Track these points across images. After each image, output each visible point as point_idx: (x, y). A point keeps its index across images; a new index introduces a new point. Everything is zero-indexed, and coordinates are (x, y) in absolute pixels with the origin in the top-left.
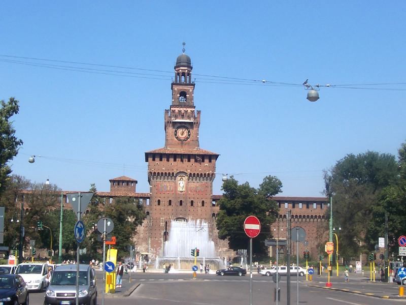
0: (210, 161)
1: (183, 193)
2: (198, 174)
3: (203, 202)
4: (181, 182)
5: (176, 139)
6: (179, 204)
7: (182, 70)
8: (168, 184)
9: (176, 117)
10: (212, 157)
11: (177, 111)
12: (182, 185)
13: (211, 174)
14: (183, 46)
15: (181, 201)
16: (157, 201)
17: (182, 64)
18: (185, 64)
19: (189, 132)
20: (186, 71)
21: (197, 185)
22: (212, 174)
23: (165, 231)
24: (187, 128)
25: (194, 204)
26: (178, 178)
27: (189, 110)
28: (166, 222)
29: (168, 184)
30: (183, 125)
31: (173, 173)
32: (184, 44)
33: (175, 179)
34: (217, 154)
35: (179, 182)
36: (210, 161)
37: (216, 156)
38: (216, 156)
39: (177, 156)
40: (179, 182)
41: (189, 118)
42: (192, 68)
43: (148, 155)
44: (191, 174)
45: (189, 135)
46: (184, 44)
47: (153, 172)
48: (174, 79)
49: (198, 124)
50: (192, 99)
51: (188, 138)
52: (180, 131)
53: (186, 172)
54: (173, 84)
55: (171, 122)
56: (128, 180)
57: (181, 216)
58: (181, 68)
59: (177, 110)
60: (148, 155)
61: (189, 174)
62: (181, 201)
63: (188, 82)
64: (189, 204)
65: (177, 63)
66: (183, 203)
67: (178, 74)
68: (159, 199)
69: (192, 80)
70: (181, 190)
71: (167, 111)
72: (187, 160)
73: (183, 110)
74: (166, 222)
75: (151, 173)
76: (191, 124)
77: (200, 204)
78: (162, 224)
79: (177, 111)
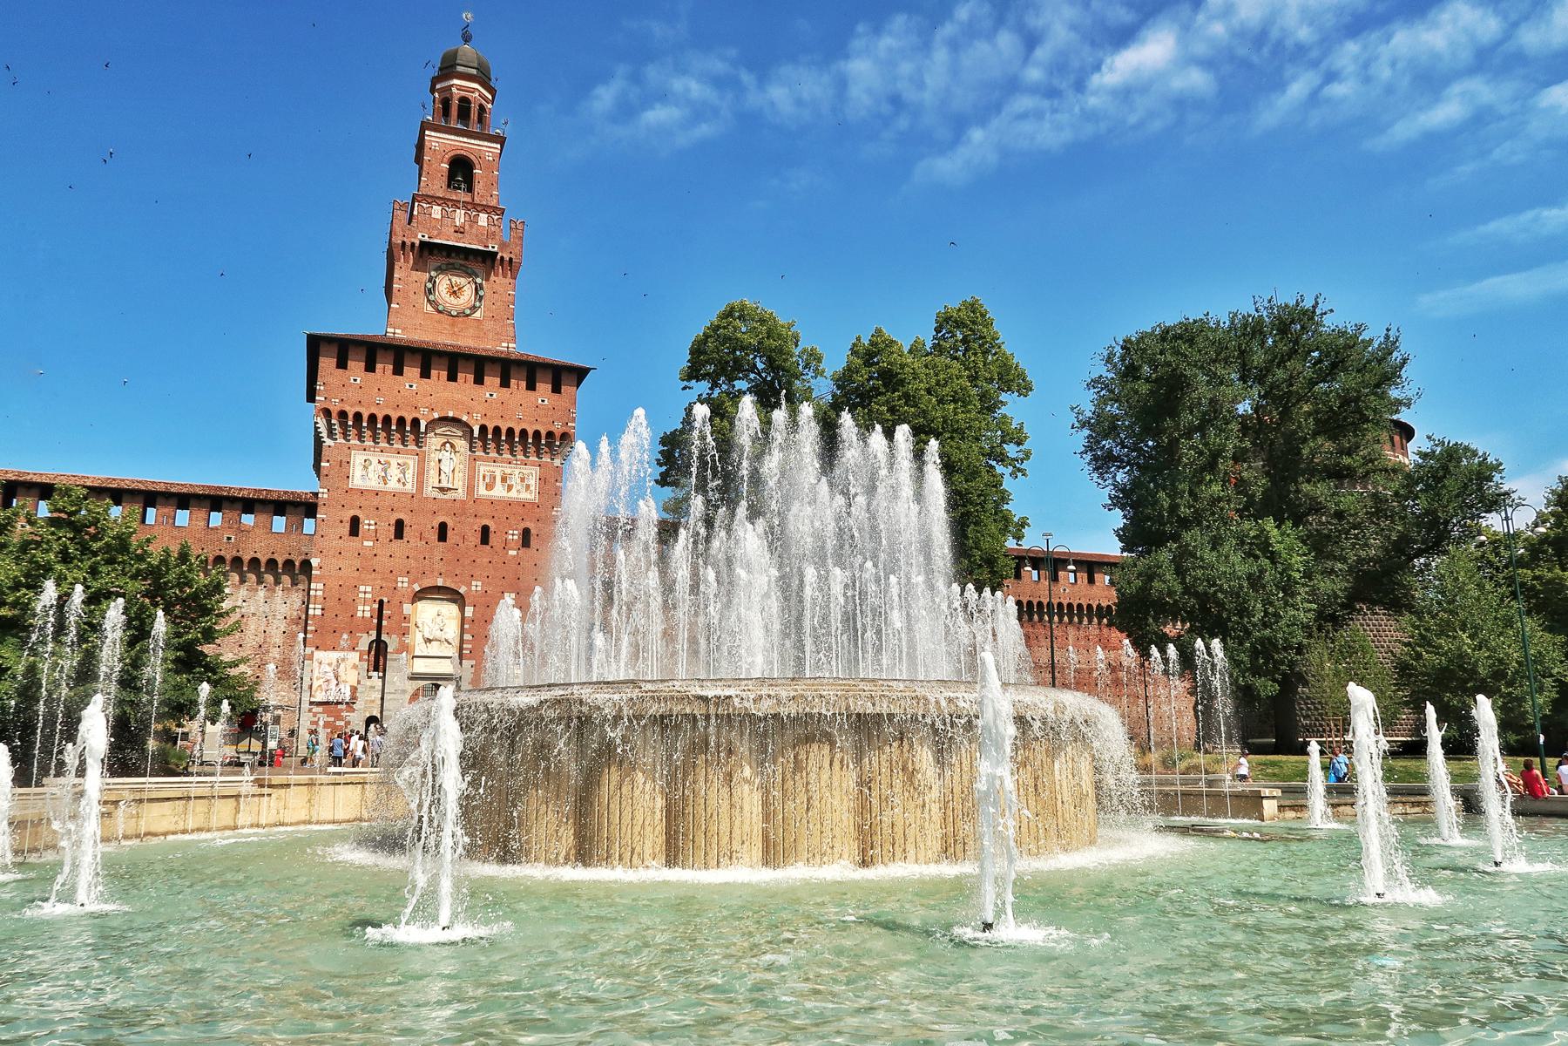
1: (449, 496)
2: (510, 431)
3: (526, 534)
4: (445, 455)
7: (460, 88)
10: (564, 376)
12: (446, 467)
13: (558, 435)
15: (443, 528)
16: (347, 518)
17: (460, 69)
19: (478, 288)
24: (470, 274)
25: (493, 538)
26: (433, 442)
27: (483, 219)
28: (381, 603)
30: (463, 262)
31: (416, 422)
33: (418, 443)
35: (436, 456)
36: (556, 389)
37: (580, 374)
38: (580, 374)
39: (435, 360)
40: (436, 456)
43: (315, 345)
44: (483, 429)
49: (511, 266)
51: (474, 308)
52: (443, 283)
53: (465, 418)
54: (424, 126)
55: (413, 244)
57: (440, 582)
58: (456, 82)
59: (436, 211)
60: (315, 345)
62: (443, 528)
64: (477, 538)
65: (440, 69)
68: (357, 513)
70: (444, 484)
72: (471, 377)
73: (460, 217)
74: (381, 603)
76: (487, 259)
77: (514, 535)
78: (365, 611)
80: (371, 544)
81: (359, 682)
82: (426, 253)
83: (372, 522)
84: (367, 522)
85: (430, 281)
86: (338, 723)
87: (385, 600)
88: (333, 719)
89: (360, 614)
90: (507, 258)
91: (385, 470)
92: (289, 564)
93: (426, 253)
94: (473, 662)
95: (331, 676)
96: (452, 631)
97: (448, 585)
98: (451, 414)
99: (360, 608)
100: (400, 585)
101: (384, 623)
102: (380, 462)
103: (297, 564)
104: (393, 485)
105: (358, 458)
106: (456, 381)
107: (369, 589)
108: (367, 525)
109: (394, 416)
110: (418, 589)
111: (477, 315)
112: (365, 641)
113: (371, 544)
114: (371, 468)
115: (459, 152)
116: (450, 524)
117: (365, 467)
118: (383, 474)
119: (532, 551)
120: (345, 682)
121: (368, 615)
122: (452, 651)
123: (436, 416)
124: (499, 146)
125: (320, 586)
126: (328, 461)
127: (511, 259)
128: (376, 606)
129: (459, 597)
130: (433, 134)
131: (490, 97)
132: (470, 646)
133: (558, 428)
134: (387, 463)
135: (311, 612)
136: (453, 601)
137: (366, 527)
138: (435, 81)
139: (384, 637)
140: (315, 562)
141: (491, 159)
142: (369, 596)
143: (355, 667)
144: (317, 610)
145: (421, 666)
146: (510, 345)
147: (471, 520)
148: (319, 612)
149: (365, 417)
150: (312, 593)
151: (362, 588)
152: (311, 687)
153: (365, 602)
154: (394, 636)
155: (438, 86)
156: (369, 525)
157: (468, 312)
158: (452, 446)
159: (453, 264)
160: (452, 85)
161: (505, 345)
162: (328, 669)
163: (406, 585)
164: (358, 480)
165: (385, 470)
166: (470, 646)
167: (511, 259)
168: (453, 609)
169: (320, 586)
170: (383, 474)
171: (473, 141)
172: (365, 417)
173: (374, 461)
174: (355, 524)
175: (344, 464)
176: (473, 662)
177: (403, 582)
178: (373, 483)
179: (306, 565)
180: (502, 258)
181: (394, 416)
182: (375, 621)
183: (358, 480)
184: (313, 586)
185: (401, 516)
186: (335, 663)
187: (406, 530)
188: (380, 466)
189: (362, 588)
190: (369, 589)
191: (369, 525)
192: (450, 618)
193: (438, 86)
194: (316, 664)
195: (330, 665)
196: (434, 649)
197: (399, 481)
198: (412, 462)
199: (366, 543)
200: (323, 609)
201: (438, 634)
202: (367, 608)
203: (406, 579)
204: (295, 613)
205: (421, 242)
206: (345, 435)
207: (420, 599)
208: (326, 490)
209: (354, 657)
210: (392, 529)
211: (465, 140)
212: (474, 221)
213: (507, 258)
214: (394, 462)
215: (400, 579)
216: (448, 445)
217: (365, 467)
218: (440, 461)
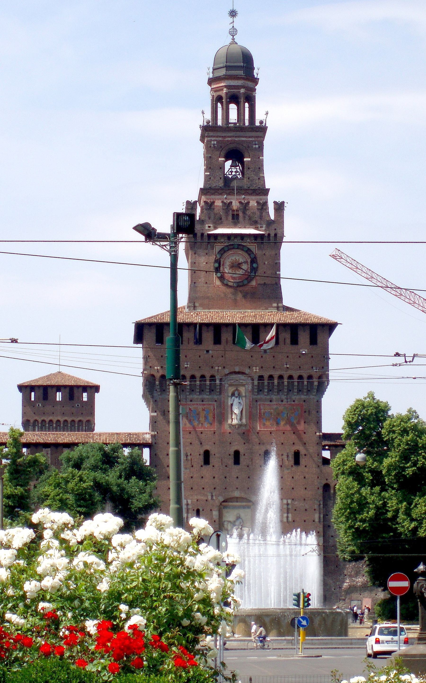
0: (313, 341)
5: (218, 283)
6: (231, 461)
8: (200, 408)
9: (218, 223)
11: (218, 203)
14: (231, 20)
15: (237, 454)
18: (241, 73)
19: (254, 260)
20: (242, 91)
21: (281, 408)
22: (320, 377)
29: (200, 408)
32: (233, 14)
34: (336, 321)
36: (313, 341)
41: (254, 224)
42: (255, 81)
44: (261, 378)
45: (254, 270)
46: (233, 14)
47: (158, 375)
48: (208, 116)
50: (260, 168)
53: (247, 371)
55: (202, 235)
56: (73, 383)
57: (237, 494)
61: (256, 378)
62: (237, 454)
63: (247, 123)
65: (214, 69)
66: (242, 459)
67: (219, 99)
69: (259, 116)
70: (235, 422)
75: (153, 376)
79: (218, 203)
82: (212, 240)
85: (216, 261)
87: (201, 510)
90: (272, 235)
93: (212, 240)
98: (237, 369)
109: (198, 375)
110: (221, 499)
111: (254, 283)
115: (232, 146)
116: (242, 452)
119: (301, 467)
123: (227, 371)
126: (156, 412)
127: (276, 235)
133: (315, 372)
146: (280, 305)
147: (257, 447)
157: (246, 282)
159: (232, 245)
161: (275, 305)
167: (276, 235)
175: (166, 413)
180: (269, 235)
181: (198, 375)
185: (208, 448)
205: (209, 236)
207: (225, 507)
210: (202, 457)
212: (245, 206)
213: (272, 235)
216: (236, 394)
218: (232, 405)
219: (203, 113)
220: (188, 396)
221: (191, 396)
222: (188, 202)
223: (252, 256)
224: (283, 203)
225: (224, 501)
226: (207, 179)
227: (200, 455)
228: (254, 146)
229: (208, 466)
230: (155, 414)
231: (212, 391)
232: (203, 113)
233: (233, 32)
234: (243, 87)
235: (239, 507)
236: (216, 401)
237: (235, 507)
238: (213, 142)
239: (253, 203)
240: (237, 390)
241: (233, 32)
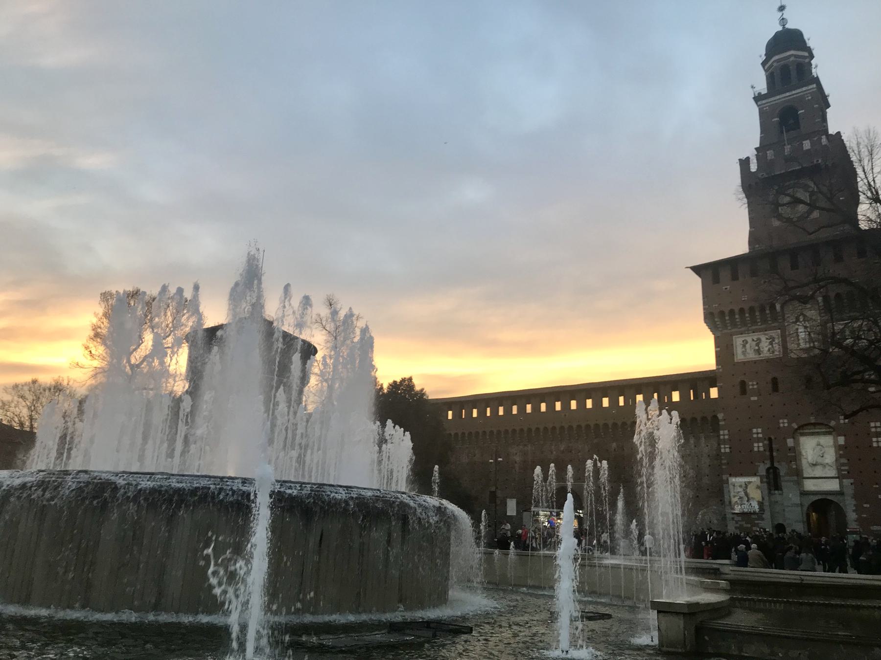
7: (778, 61)
23: (768, 465)
27: (807, 145)
28: (770, 439)
46: (782, 8)
71: (744, 163)
74: (770, 439)
78: (759, 447)
80: (756, 398)
81: (763, 499)
83: (755, 383)
84: (750, 383)
86: (754, 528)
87: (773, 438)
88: (749, 526)
89: (756, 449)
91: (757, 345)
92: (704, 419)
94: (852, 481)
95: (742, 494)
96: (830, 457)
97: (819, 421)
99: (756, 445)
100: (781, 425)
101: (775, 454)
102: (753, 340)
103: (709, 419)
104: (766, 353)
105: (738, 341)
106: (797, 268)
107: (760, 430)
108: (752, 385)
110: (795, 426)
112: (762, 469)
113: (756, 398)
114: (748, 346)
117: (744, 346)
118: (757, 348)
120: (753, 499)
121: (762, 449)
122: (833, 473)
124: (814, 86)
125: (726, 432)
128: (766, 442)
129: (831, 430)
130: (764, 102)
131: (806, 54)
132: (846, 468)
134: (759, 340)
135: (723, 450)
136: (829, 433)
137: (751, 387)
138: (764, 64)
139: (776, 465)
140: (720, 416)
141: (810, 98)
142: (760, 436)
143: (758, 487)
144: (725, 449)
145: (810, 485)
148: (728, 450)
149: (727, 312)
150: (722, 437)
151: (755, 430)
152: (730, 502)
153: (758, 440)
154: (783, 463)
155: (766, 67)
156: (753, 385)
157: (806, 215)
158: (805, 316)
160: (774, 62)
162: (740, 489)
163: (786, 425)
164: (739, 357)
165: (757, 345)
166: (846, 468)
168: (827, 441)
169: (726, 432)
170: (757, 348)
171: (794, 92)
172: (737, 311)
173: (749, 339)
174: (743, 384)
176: (852, 481)
177: (784, 423)
178: (752, 356)
179: (715, 417)
182: (768, 453)
183: (739, 357)
184: (721, 432)
186: (744, 485)
187: (780, 386)
188: (754, 343)
189: (755, 430)
190: (760, 430)
191: (753, 385)
192: (828, 447)
193: (766, 67)
194: (731, 487)
195: (741, 486)
196: (818, 472)
197: (769, 350)
198: (776, 333)
199: (753, 399)
200: (730, 448)
201: (820, 460)
202: (761, 444)
203: (786, 421)
204: (715, 452)
206: (725, 327)
207: (803, 434)
208: (720, 367)
209: (755, 480)
210: (770, 385)
211: (788, 94)
214: (763, 338)
215: (781, 421)
216: (801, 319)
217: (744, 346)
219: (753, 87)
220: (750, 328)
221: (754, 327)
222: (740, 160)
223: (811, 190)
224: (839, 133)
225: (797, 429)
226: (762, 139)
227: (767, 383)
228: (807, 98)
229: (777, 393)
230: (718, 349)
231: (775, 319)
232: (753, 87)
233: (783, 21)
234: (792, 55)
235: (818, 434)
236: (779, 329)
237: (813, 434)
238: (765, 109)
239: (807, 145)
240: (802, 314)
241: (783, 21)
